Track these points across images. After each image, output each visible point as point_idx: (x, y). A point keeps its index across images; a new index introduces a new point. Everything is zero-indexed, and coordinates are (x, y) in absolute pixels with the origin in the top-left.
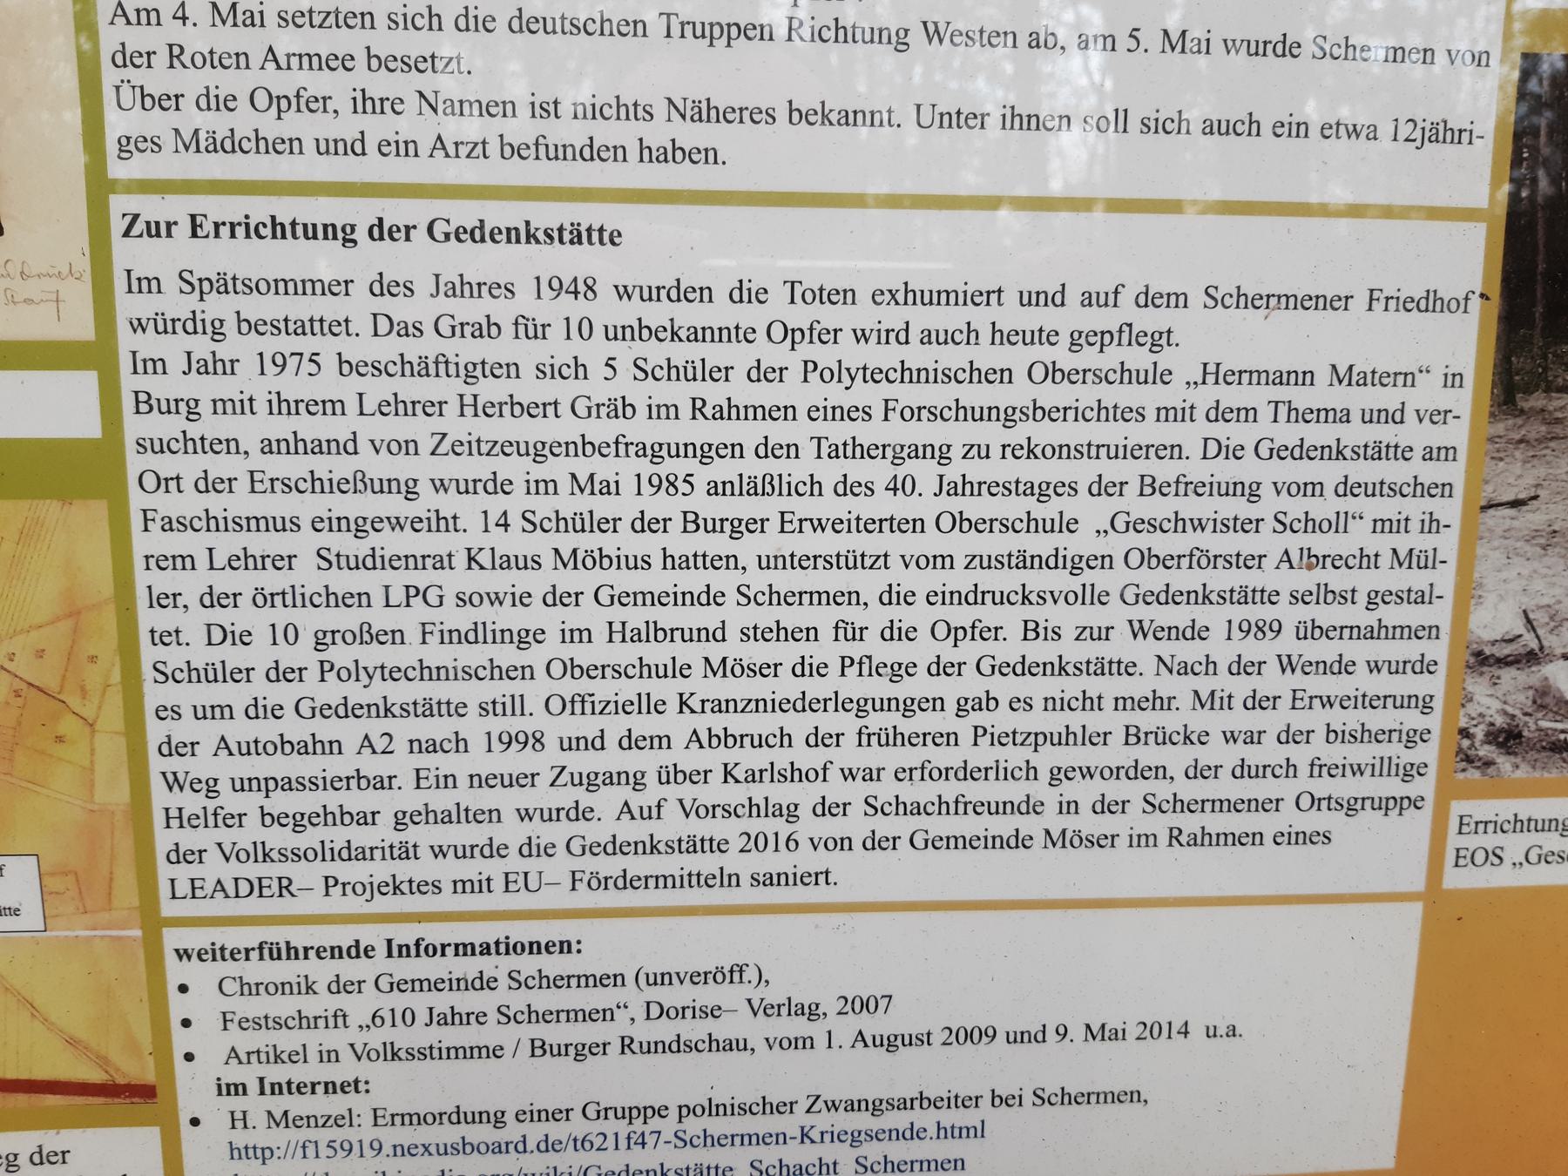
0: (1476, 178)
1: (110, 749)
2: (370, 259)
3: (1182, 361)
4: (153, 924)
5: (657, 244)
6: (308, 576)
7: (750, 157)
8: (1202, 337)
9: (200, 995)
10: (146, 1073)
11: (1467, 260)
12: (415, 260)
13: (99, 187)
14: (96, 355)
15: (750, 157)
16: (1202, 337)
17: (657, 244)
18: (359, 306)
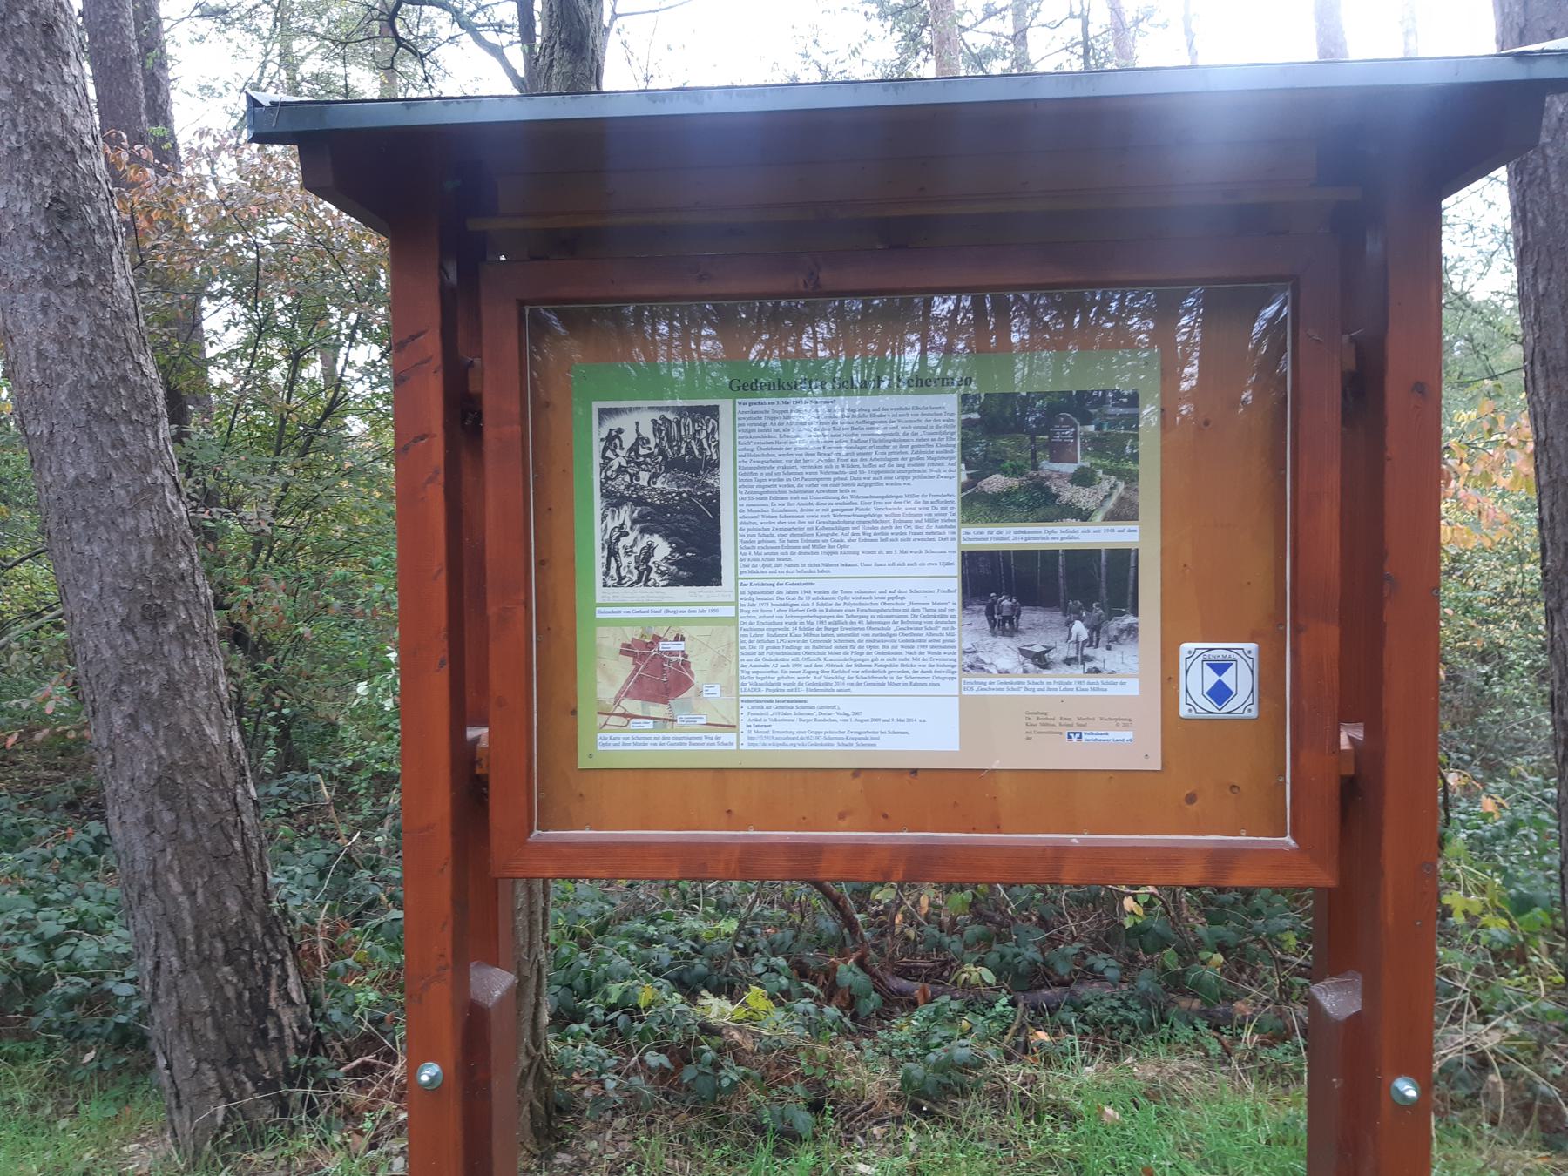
0: (955, 570)
1: (733, 665)
2: (777, 588)
3: (907, 602)
4: (738, 696)
5: (820, 585)
6: (765, 638)
7: (834, 572)
8: (909, 598)
9: (745, 708)
10: (733, 722)
11: (955, 584)
12: (783, 589)
13: (737, 579)
14: (735, 604)
15: (834, 572)
16: (909, 598)
17: (820, 585)
18: (774, 596)
